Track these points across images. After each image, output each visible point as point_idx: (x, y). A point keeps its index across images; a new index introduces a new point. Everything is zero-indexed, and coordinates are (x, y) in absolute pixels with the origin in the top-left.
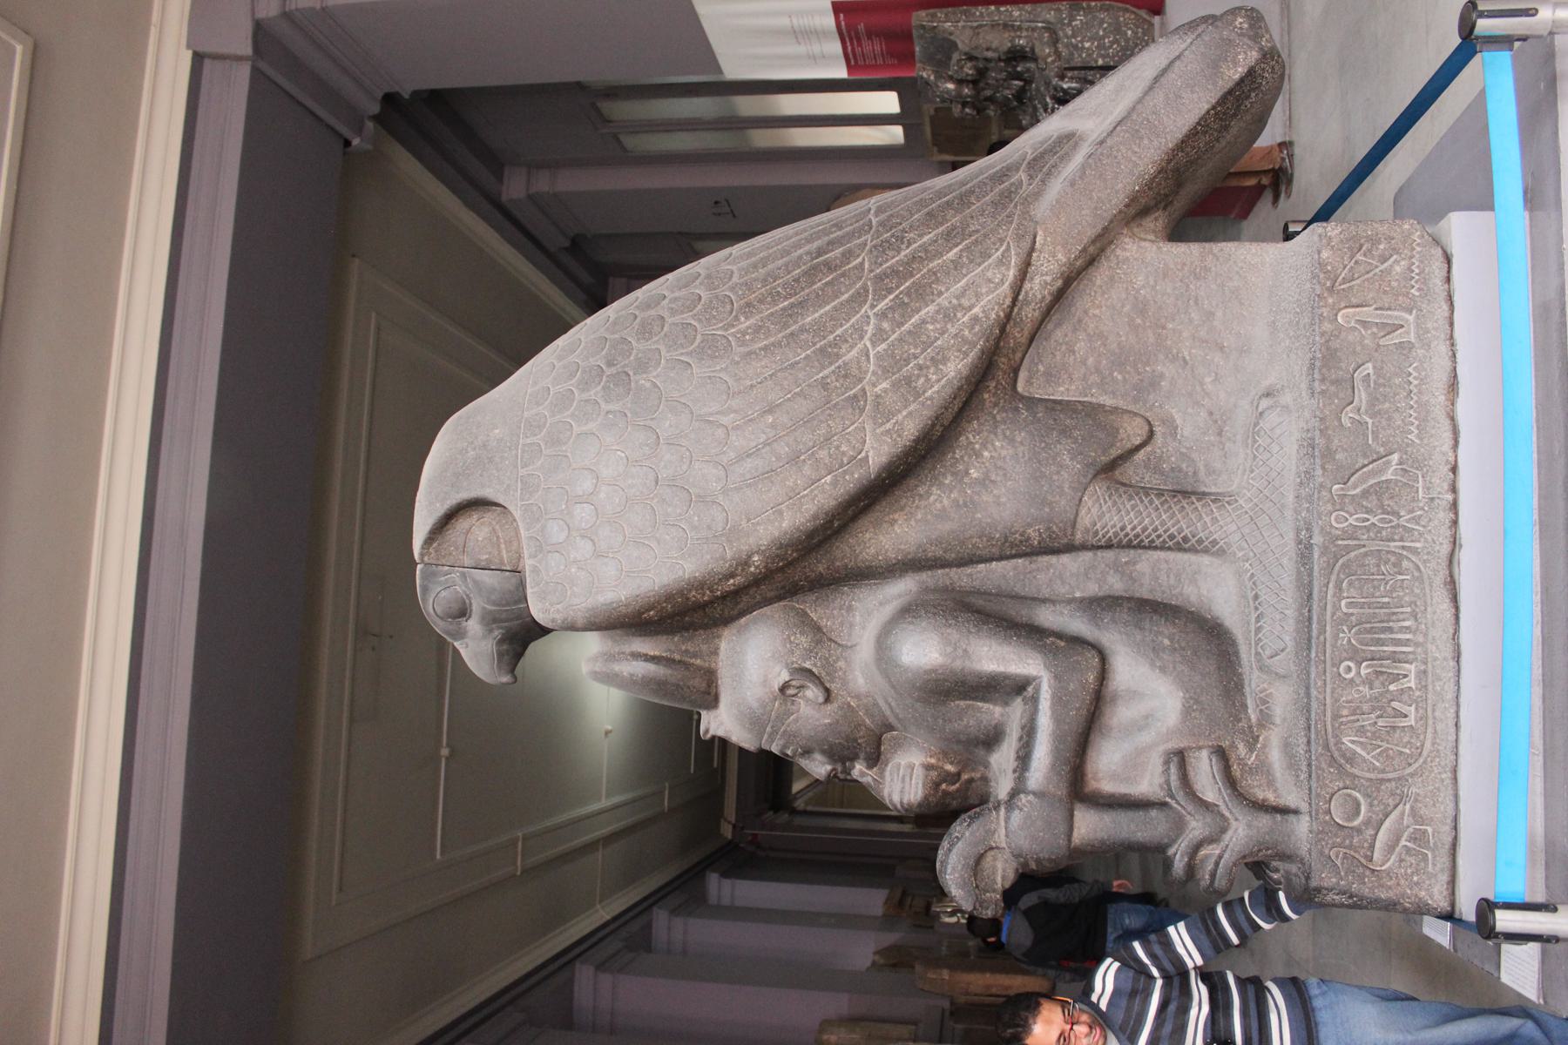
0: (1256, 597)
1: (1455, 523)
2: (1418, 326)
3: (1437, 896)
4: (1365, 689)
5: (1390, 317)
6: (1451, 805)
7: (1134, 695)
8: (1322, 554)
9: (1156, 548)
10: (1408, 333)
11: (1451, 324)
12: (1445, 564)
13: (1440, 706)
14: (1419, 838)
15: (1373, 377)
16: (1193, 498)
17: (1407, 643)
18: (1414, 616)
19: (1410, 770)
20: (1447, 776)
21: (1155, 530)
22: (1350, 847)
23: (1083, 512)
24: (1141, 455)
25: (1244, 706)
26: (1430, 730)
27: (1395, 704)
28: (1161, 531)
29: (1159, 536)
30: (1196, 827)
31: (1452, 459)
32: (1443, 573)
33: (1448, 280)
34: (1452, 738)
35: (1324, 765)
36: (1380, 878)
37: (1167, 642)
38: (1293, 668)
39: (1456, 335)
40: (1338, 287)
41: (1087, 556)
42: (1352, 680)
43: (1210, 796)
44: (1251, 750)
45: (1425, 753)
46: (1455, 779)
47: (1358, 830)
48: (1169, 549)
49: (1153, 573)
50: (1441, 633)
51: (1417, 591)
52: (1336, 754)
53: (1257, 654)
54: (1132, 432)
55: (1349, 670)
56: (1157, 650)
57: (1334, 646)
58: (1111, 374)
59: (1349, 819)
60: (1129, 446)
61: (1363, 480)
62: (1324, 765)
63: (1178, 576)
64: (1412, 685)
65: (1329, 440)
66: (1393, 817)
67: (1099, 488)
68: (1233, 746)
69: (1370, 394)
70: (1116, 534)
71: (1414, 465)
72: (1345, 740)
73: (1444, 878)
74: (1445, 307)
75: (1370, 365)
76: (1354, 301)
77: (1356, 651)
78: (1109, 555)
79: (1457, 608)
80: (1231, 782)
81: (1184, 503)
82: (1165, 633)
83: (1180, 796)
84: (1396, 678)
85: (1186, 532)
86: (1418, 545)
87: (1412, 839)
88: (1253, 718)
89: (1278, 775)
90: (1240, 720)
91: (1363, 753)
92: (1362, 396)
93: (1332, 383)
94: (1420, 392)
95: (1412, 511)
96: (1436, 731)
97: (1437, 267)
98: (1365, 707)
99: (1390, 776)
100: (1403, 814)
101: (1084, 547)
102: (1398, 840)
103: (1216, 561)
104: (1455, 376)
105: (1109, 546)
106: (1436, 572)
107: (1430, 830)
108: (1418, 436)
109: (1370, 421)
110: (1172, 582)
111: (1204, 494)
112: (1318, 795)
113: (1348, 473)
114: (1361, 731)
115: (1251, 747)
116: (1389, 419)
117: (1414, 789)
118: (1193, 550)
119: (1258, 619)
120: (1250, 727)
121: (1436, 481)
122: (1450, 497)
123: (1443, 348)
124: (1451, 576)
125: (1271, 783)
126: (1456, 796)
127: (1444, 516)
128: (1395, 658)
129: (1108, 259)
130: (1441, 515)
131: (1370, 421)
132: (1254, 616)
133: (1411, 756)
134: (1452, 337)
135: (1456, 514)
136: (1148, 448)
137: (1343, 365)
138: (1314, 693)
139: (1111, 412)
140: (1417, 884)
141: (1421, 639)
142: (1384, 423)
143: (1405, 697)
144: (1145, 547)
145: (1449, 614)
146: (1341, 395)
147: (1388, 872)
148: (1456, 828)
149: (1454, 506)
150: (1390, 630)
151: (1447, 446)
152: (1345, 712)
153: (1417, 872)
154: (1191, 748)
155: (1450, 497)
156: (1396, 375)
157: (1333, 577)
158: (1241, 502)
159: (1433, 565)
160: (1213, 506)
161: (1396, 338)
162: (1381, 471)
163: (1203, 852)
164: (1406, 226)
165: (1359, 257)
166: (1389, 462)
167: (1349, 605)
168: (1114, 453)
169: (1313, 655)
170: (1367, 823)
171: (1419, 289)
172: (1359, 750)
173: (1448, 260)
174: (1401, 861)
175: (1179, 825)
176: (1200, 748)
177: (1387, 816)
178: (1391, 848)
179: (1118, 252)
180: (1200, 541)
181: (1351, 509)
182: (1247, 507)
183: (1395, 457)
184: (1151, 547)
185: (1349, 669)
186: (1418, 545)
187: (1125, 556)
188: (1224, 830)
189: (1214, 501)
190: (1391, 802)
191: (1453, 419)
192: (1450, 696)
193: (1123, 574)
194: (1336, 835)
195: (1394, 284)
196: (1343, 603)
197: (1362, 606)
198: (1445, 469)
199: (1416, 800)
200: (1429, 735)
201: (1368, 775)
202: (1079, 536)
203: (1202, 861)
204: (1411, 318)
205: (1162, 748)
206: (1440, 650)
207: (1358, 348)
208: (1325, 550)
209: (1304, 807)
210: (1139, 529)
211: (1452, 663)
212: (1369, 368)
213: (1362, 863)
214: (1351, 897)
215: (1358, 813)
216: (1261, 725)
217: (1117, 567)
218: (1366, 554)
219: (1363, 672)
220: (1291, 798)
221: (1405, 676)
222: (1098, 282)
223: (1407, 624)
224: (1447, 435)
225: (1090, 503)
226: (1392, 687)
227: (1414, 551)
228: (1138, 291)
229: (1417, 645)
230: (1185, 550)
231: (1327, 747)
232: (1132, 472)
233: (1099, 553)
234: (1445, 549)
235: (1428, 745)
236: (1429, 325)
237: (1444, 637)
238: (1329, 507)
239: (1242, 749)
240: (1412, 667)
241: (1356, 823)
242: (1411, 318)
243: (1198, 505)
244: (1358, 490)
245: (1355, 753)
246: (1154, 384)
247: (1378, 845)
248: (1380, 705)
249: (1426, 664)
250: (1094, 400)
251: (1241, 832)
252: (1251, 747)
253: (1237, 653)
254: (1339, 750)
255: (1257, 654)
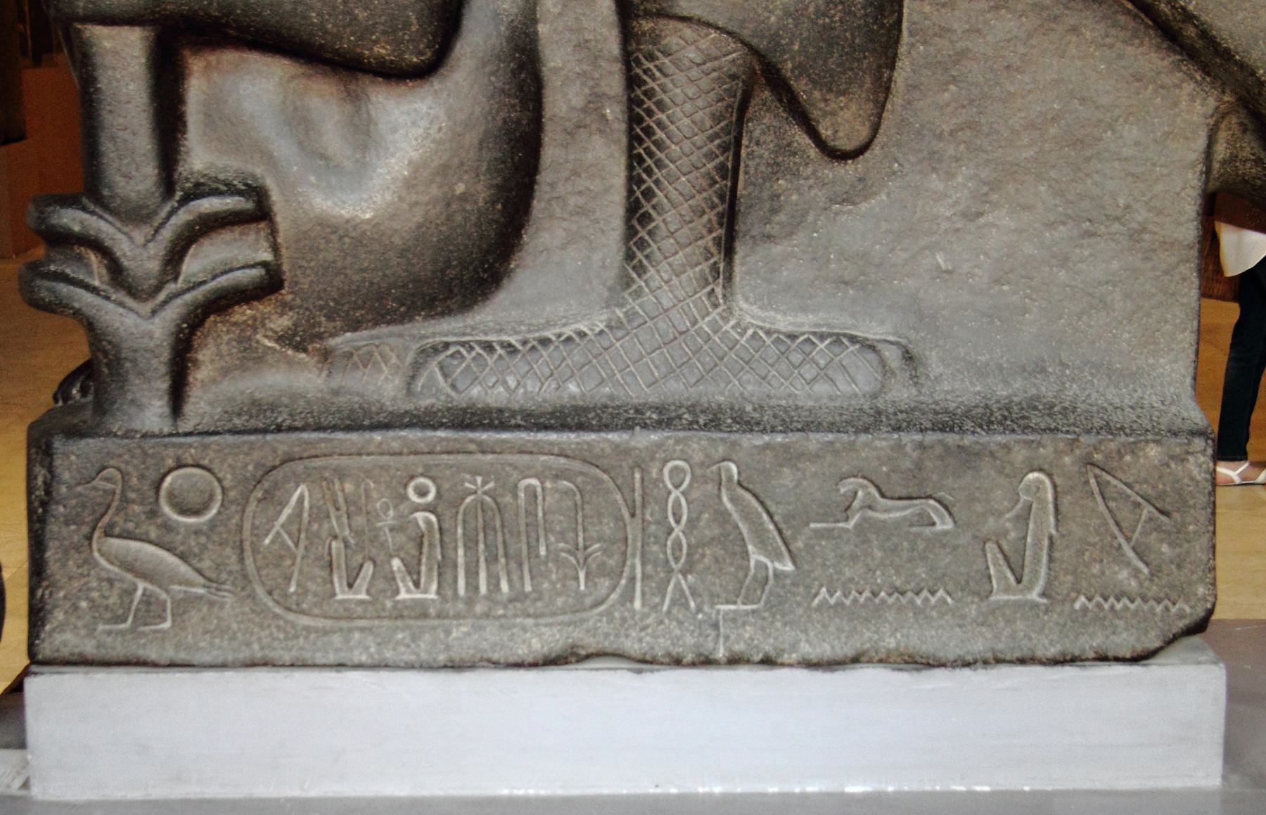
0: (545, 342)
1: (677, 662)
2: (1018, 605)
3: (59, 638)
4: (390, 517)
5: (1036, 559)
6: (207, 658)
7: (363, 135)
8: (616, 447)
9: (630, 168)
10: (1007, 590)
11: (1022, 661)
12: (607, 645)
13: (370, 641)
14: (151, 609)
15: (927, 531)
16: (720, 232)
17: (473, 587)
18: (518, 597)
19: (260, 591)
20: (257, 652)
21: (659, 164)
22: (125, 500)
23: (688, 32)
24: (801, 139)
25: (355, 326)
26: (329, 623)
27: (369, 569)
28: (658, 174)
29: (649, 171)
30: (140, 251)
31: (786, 658)
32: (592, 643)
33: (1103, 658)
34: (319, 658)
35: (256, 455)
36: (77, 548)
37: (460, 188)
38: (425, 403)
39: (1004, 670)
40: (1092, 472)
41: (613, 46)
42: (405, 498)
43: (193, 265)
44: (280, 339)
45: (291, 617)
46: (252, 664)
47: (153, 513)
48: (630, 192)
49: (583, 169)
50: (490, 638)
51: (560, 601)
52: (278, 474)
53: (447, 345)
54: (844, 120)
55: (422, 492)
56: (444, 169)
57: (460, 468)
58: (954, 80)
59: (171, 496)
60: (815, 114)
61: (747, 514)
62: (256, 455)
63: (581, 211)
64: (403, 595)
65: (817, 457)
66: (183, 568)
67: (734, 55)
68: (285, 307)
69: (897, 524)
70: (650, 94)
71: (776, 598)
72: (302, 489)
73: (89, 648)
74: (1053, 652)
75: (949, 525)
76: (1066, 501)
77: (456, 504)
78: (614, 84)
79: (534, 665)
80: (221, 303)
81: (711, 215)
82: (475, 189)
83: (183, 216)
84: (413, 571)
85: (658, 220)
86: (637, 604)
87: (148, 599)
88: (332, 342)
89: (241, 385)
90: (330, 318)
91: (283, 518)
92: (896, 513)
93: (919, 466)
94: (901, 609)
95: (694, 593)
96: (326, 632)
97: (1125, 641)
98: (359, 521)
99: (249, 561)
100: (190, 583)
101: (627, 35)
102: (144, 576)
103: (611, 275)
104: (929, 666)
105: (632, 81)
106: (593, 632)
107: (167, 625)
108: (825, 603)
109: (850, 525)
110: (573, 201)
111: (729, 252)
112: (206, 447)
113: (757, 488)
114: (320, 515)
115: (284, 339)
116: (854, 558)
117: (229, 600)
118: (630, 232)
119: (508, 347)
120: (320, 336)
121: (748, 631)
122: (721, 654)
123: (978, 646)
124: (588, 657)
125: (225, 372)
126: (224, 666)
127: (687, 643)
128: (445, 568)
129: (1177, 66)
130: (690, 640)
131: (850, 525)
132: (513, 340)
133: (286, 595)
134: (999, 661)
135: (693, 665)
136: (813, 152)
137: (949, 481)
138: (377, 437)
139: (877, 79)
140: (76, 608)
141: (479, 609)
142: (847, 549)
143: (381, 584)
144: (631, 148)
145: (522, 652)
146: (894, 477)
147: (89, 562)
148: (173, 665)
149: (706, 662)
150: (492, 560)
151: (806, 649)
152: (349, 487)
153: (94, 606)
154: (274, 232)
155: (721, 654)
156: (932, 569)
157: (577, 465)
158: (715, 314)
159: (604, 626)
160: (705, 266)
161: (997, 569)
162: (763, 543)
163: (93, 258)
164: (1201, 590)
165: (1147, 510)
166: (778, 557)
167: (532, 494)
168: (801, 86)
169: (441, 434)
170: (167, 527)
171: (1085, 610)
172: (287, 511)
173: (1138, 659)
174: (111, 582)
175: (134, 215)
176: (275, 248)
177: (183, 557)
178: (129, 566)
179: (1189, 87)
180: (642, 244)
181: (695, 495)
182: (704, 325)
183: (789, 567)
184: (634, 160)
185: (422, 492)
186: (637, 604)
187: (614, 112)
188: (133, 292)
189: (715, 268)
190: (206, 564)
191: (856, 660)
192: (389, 654)
193: (584, 110)
194: (142, 477)
195: (1096, 569)
196: (534, 482)
197: (531, 513)
198: (768, 647)
199: (212, 604)
200: (320, 623)
201: (247, 525)
202: (646, 25)
203: (79, 258)
204: (1034, 596)
205: (270, 183)
206: (463, 639)
207: (979, 508)
208: (622, 451)
209: (185, 426)
210: (660, 134)
211: (442, 658)
212: (944, 524)
213: (99, 521)
214: (44, 504)
215: (184, 511)
216: (326, 356)
217: (595, 102)
218: (619, 518)
219: (420, 516)
220: (199, 406)
221: (417, 584)
222: (1130, 50)
223: (504, 586)
224: (825, 650)
225: (704, 44)
226: (396, 563)
227: (628, 597)
228: (1111, 127)
229: (470, 602)
230: (628, 220)
231: (289, 459)
232: (767, 127)
233: (617, 67)
234: (631, 645)
235: (304, 621)
236: (1020, 625)
237: (485, 645)
238: (698, 457)
239: (282, 323)
240: (432, 595)
241: (167, 509)
242: (1034, 596)
243: (708, 241)
244: (729, 506)
245: (283, 504)
246: (934, 161)
247: (134, 545)
248: (367, 546)
249: (439, 616)
250: (903, 49)
251: (143, 328)
252: (284, 339)
253: (447, 312)
254: (286, 479)
255: (447, 345)
